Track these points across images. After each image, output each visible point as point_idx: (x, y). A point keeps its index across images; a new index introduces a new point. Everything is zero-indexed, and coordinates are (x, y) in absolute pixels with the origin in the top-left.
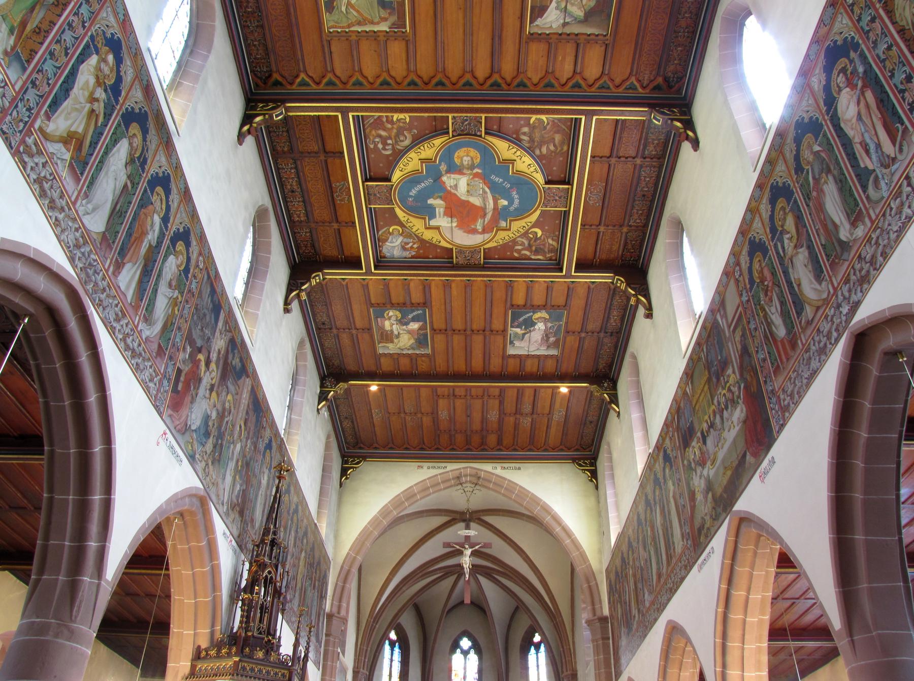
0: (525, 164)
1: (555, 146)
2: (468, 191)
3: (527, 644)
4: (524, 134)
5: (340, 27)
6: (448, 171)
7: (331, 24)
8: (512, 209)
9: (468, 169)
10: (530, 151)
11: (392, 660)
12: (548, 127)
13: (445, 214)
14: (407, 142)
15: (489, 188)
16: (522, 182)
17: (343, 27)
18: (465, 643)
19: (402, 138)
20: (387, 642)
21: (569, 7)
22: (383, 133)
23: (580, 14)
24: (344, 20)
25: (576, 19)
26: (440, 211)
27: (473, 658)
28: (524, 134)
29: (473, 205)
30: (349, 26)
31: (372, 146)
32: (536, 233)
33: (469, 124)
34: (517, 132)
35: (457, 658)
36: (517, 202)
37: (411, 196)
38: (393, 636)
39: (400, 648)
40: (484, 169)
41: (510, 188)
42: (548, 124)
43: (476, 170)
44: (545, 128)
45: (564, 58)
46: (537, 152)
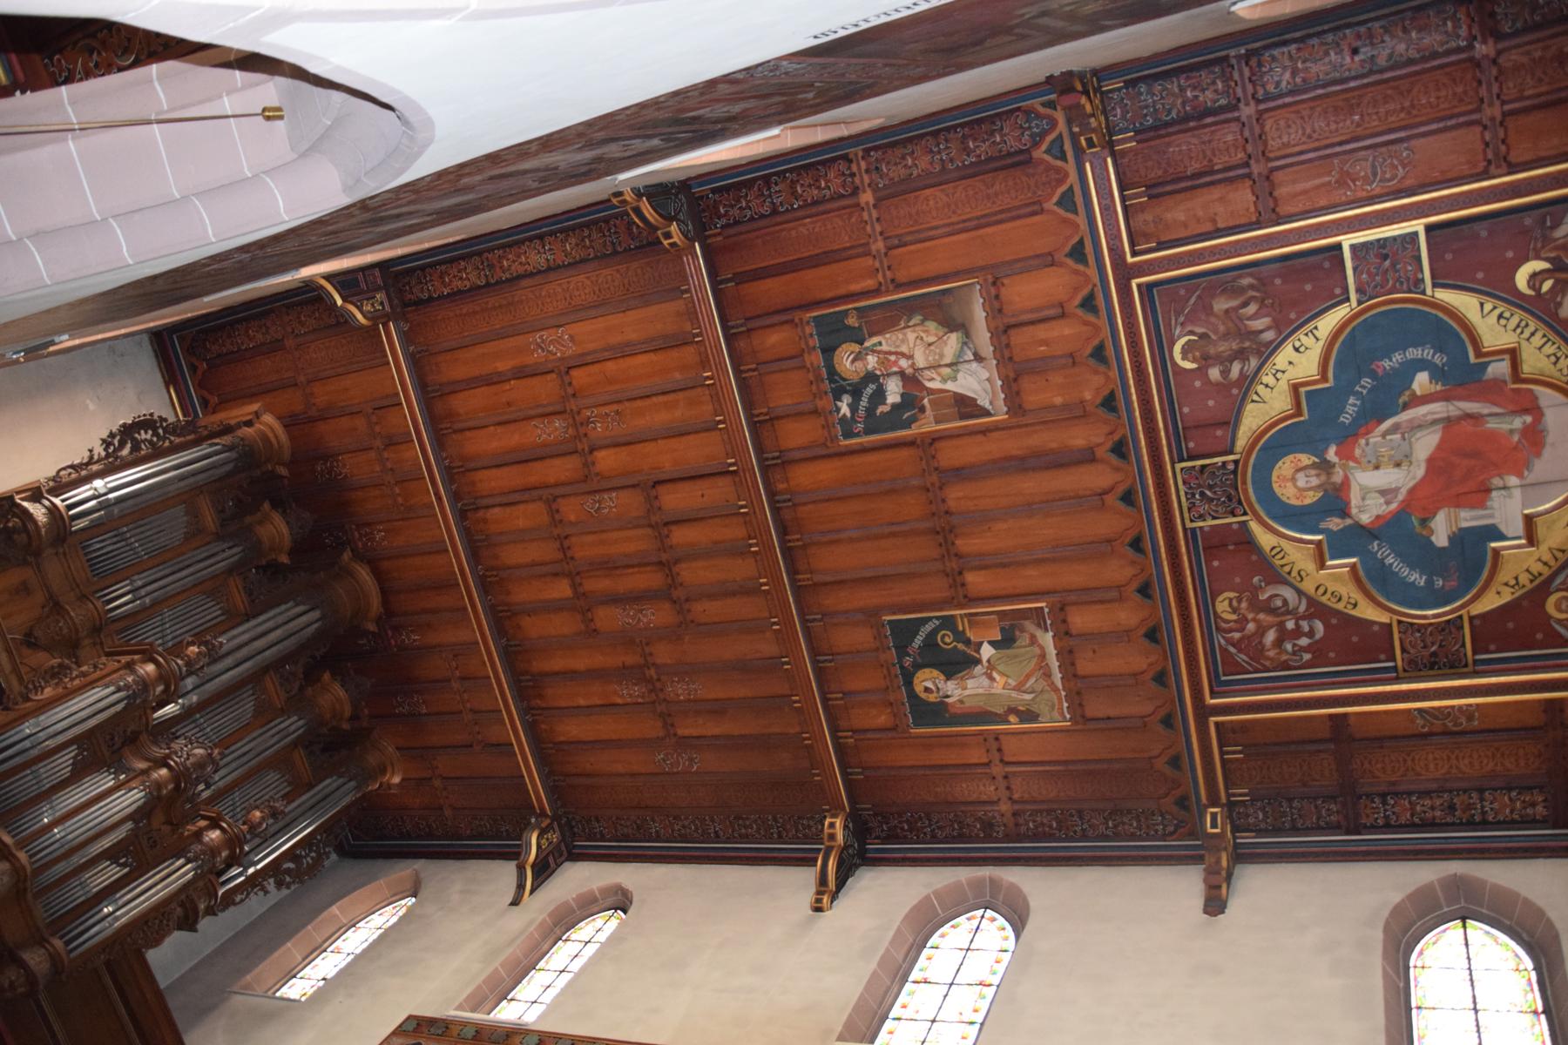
0: (1301, 359)
1: (1245, 304)
2: (1398, 465)
4: (1225, 373)
5: (1060, 703)
6: (1344, 512)
7: (1056, 715)
8: (1438, 359)
9: (1329, 474)
10: (1267, 352)
12: (1200, 330)
13: (1481, 505)
14: (1288, 593)
15: (1380, 422)
16: (1349, 353)
17: (1060, 699)
19: (1279, 603)
21: (947, 360)
22: (1271, 636)
23: (954, 339)
24: (1046, 696)
25: (965, 343)
26: (1468, 518)
28: (1225, 373)
29: (1439, 447)
30: (1056, 690)
31: (1307, 657)
32: (1534, 276)
33: (1210, 487)
34: (1223, 388)
36: (1413, 353)
37: (1429, 582)
40: (1327, 442)
41: (1373, 375)
42: (1192, 333)
43: (1331, 454)
44: (1202, 336)
45: (1045, 342)
46: (1269, 336)
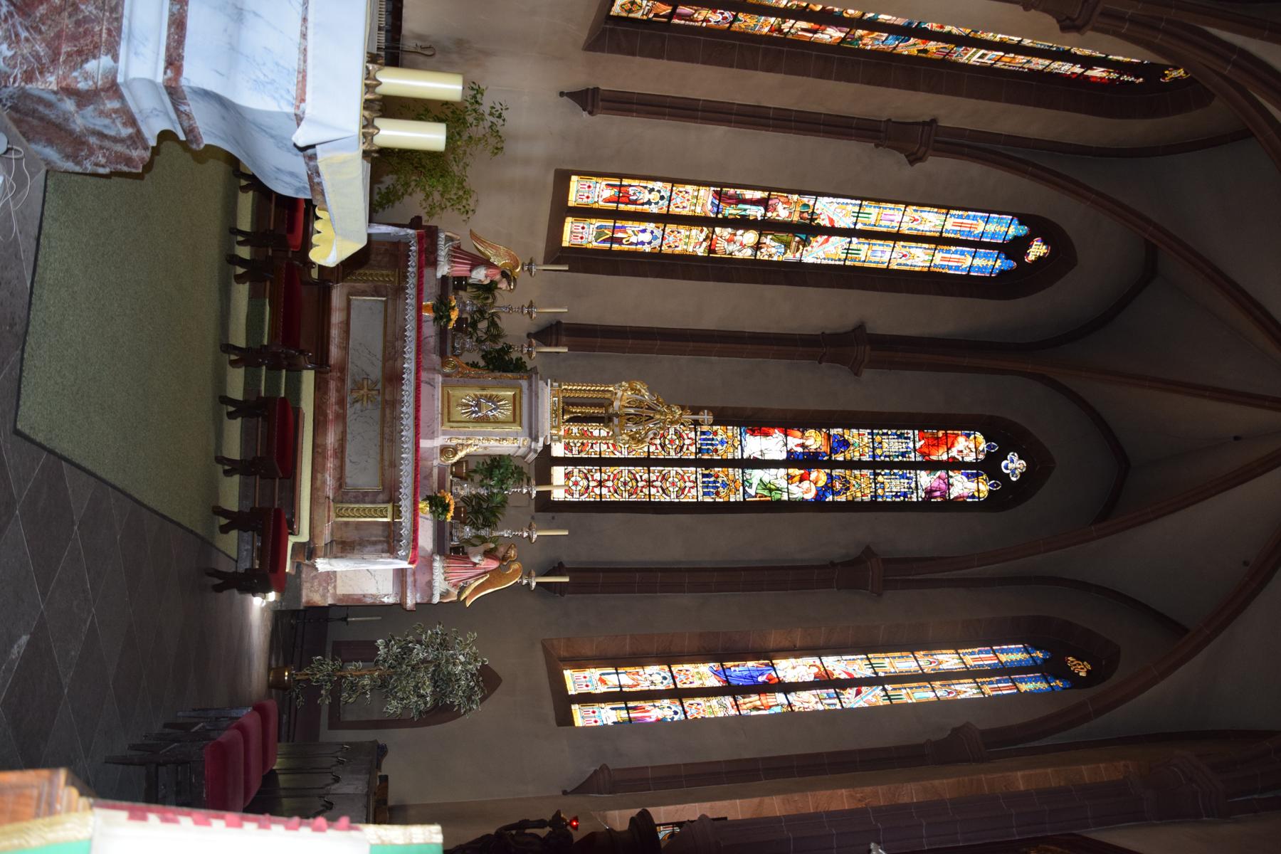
3: (1053, 642)
11: (977, 245)
18: (1014, 465)
20: (1023, 230)
27: (982, 488)
35: (968, 446)
38: (1037, 250)
39: (1002, 272)
